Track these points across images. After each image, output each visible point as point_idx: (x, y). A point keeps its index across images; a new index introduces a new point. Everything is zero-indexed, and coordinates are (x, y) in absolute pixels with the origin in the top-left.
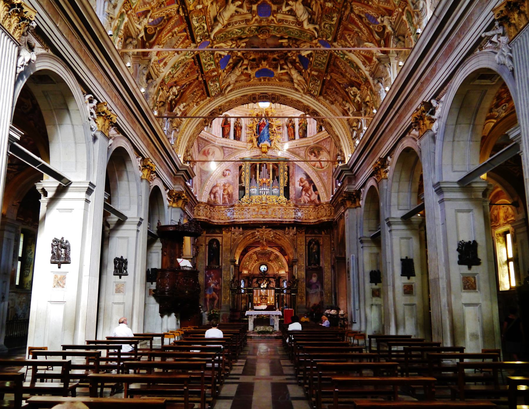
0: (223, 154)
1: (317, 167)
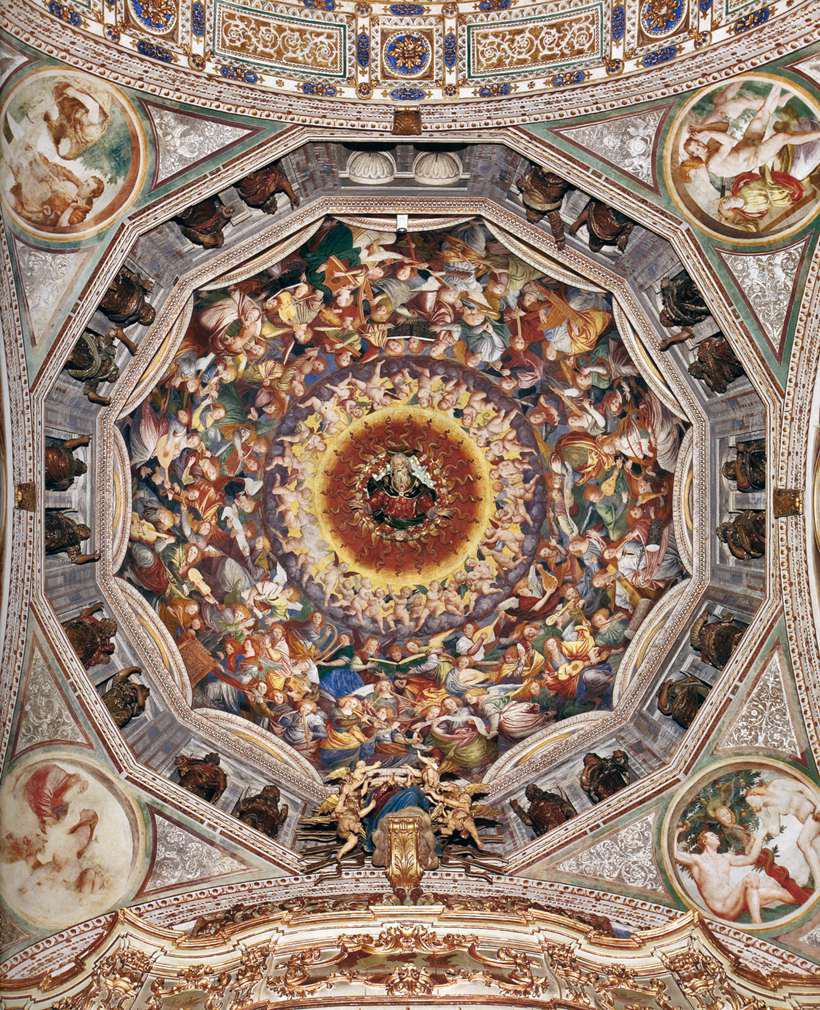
0: (142, 864)
1: (767, 913)
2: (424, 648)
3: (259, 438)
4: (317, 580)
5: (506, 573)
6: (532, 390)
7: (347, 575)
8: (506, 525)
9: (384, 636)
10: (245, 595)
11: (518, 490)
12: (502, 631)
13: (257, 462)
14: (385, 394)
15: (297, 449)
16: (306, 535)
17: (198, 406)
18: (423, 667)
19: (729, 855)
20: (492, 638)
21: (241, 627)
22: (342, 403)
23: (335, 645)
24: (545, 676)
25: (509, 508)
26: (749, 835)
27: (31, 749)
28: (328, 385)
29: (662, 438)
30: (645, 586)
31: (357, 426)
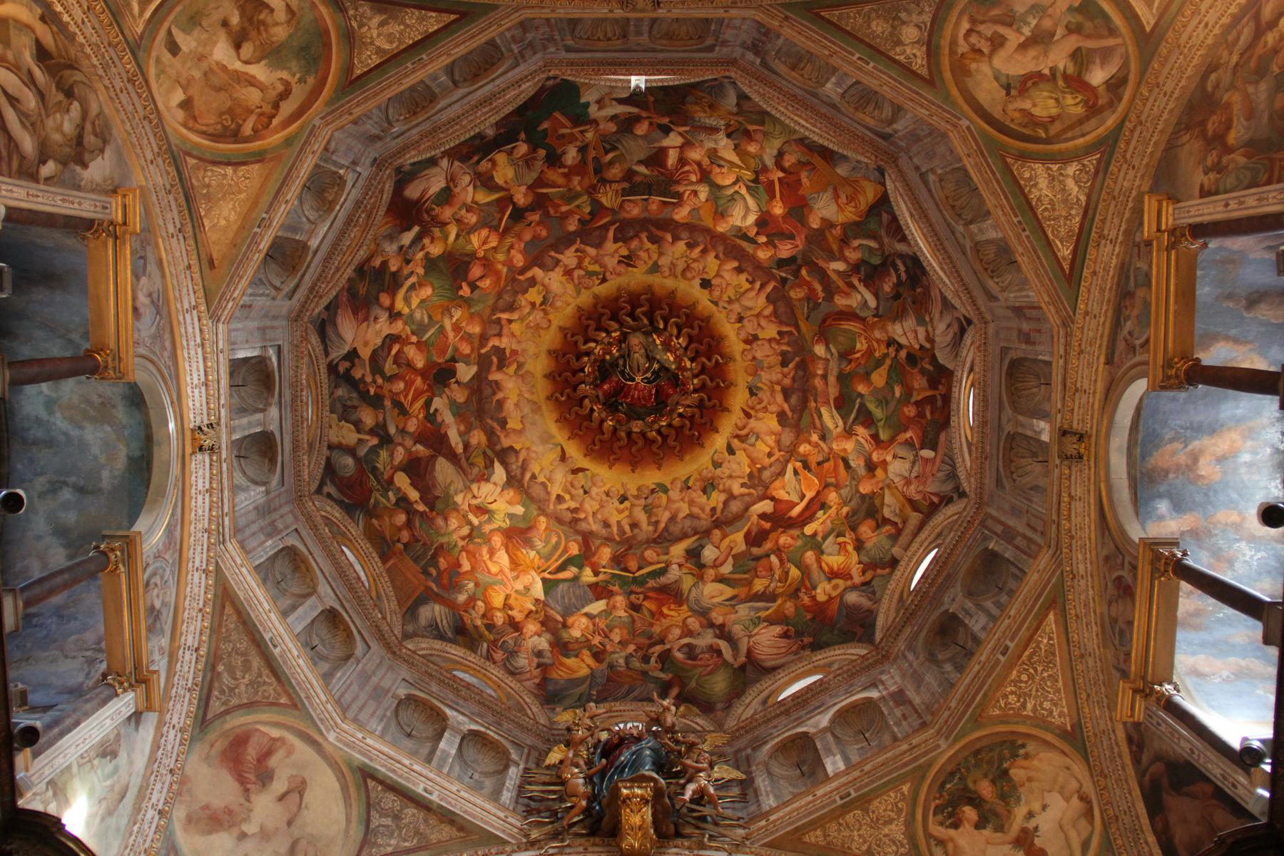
0: (357, 832)
2: (664, 558)
3: (472, 316)
4: (541, 479)
5: (760, 470)
6: (792, 260)
7: (575, 471)
8: (761, 415)
9: (618, 543)
10: (459, 499)
11: (775, 375)
12: (755, 539)
13: (471, 343)
14: (620, 262)
15: (515, 327)
16: (528, 426)
17: (401, 286)
18: (663, 580)
19: (986, 832)
20: (741, 546)
21: (455, 537)
22: (568, 273)
23: (560, 556)
24: (801, 595)
25: (765, 396)
26: (1009, 812)
27: (227, 712)
28: (553, 254)
29: (942, 330)
30: (917, 497)
31: (585, 299)
